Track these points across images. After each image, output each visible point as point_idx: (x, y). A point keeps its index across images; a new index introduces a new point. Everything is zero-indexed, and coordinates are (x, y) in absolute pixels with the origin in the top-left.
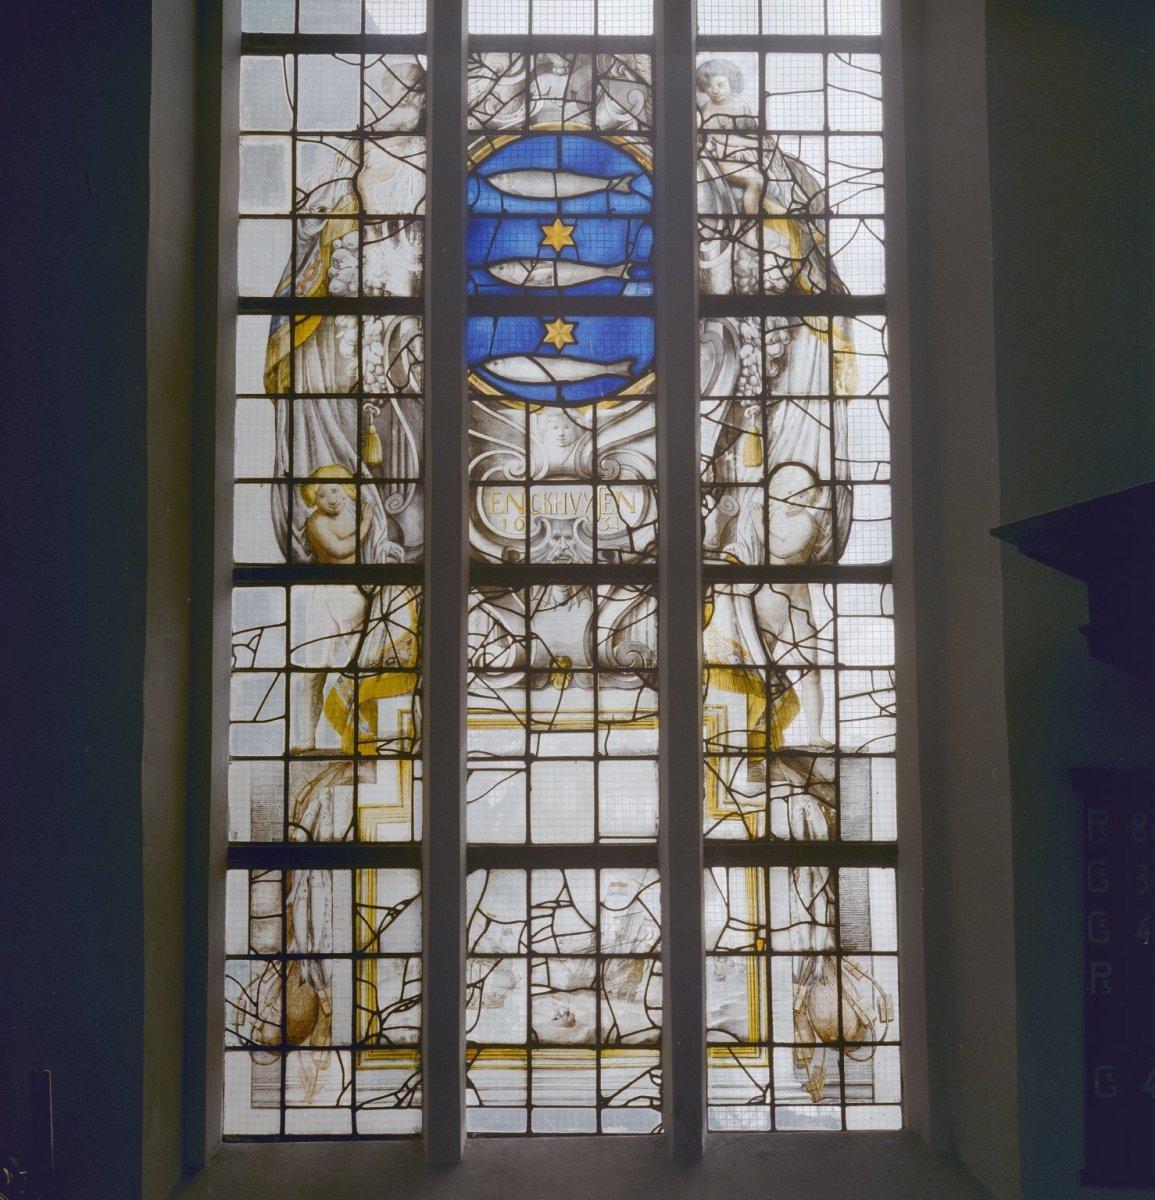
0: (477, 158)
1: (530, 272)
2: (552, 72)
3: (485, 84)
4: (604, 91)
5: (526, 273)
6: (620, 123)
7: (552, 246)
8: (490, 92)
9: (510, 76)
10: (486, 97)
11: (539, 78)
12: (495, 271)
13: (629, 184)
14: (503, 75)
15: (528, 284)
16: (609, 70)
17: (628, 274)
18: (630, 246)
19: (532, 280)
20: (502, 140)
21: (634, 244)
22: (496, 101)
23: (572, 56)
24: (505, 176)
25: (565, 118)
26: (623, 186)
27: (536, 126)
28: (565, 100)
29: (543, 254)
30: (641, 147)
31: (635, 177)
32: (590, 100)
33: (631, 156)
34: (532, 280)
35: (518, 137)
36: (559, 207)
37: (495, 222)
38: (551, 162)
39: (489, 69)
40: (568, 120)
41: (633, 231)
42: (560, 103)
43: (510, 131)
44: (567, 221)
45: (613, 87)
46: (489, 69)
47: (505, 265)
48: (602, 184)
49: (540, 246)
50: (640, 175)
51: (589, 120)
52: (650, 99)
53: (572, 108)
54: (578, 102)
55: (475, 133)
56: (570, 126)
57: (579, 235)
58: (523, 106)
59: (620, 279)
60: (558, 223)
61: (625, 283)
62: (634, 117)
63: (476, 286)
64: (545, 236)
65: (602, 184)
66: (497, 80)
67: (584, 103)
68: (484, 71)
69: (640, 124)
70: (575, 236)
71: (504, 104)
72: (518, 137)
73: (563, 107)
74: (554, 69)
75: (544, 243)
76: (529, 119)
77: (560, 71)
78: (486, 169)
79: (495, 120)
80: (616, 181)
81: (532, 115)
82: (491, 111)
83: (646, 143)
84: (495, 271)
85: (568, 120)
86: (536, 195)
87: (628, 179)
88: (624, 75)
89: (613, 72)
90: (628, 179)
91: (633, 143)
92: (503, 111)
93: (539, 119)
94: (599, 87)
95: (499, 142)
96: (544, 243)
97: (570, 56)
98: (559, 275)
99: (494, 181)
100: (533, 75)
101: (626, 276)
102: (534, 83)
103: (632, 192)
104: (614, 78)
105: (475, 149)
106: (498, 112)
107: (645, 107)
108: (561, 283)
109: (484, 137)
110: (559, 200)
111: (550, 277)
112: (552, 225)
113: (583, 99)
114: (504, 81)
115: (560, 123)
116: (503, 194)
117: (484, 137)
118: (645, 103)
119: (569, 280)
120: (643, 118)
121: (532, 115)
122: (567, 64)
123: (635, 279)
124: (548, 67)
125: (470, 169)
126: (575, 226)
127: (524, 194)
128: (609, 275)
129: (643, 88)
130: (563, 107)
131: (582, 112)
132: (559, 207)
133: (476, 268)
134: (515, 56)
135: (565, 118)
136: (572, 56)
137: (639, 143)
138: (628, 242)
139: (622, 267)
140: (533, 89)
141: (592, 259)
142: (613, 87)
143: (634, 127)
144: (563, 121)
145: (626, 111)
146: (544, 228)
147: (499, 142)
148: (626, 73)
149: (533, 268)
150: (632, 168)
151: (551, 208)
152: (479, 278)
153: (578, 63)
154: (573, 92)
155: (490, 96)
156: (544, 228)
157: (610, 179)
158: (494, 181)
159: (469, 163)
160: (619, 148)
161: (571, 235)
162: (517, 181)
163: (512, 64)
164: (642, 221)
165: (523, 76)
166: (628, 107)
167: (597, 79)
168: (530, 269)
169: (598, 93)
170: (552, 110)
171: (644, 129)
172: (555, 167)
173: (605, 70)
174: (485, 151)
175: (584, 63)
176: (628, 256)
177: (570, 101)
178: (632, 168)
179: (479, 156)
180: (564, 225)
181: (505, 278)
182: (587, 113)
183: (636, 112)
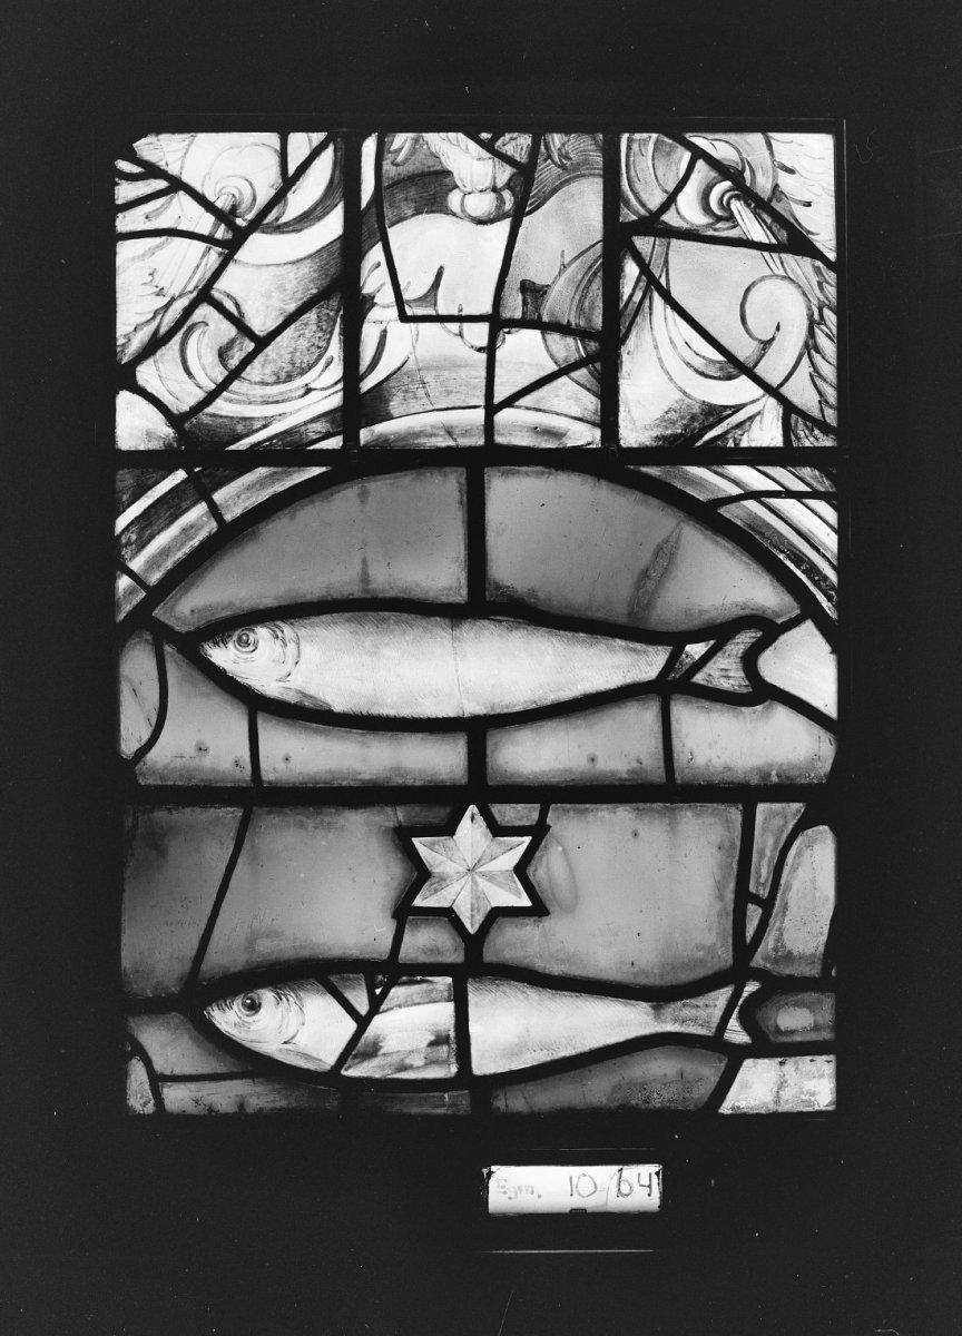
0: (153, 564)
1: (363, 1022)
2: (446, 211)
3: (183, 264)
4: (652, 283)
5: (350, 1026)
6: (715, 414)
7: (448, 915)
8: (205, 295)
9: (279, 229)
10: (188, 311)
11: (395, 234)
12: (228, 1018)
13: (749, 661)
14: (255, 225)
15: (354, 1071)
16: (671, 199)
17: (747, 1023)
18: (754, 914)
19: (372, 1051)
20: (262, 483)
21: (767, 905)
22: (230, 330)
23: (525, 140)
24: (262, 633)
25: (498, 398)
26: (724, 671)
27: (382, 428)
28: (497, 323)
29: (422, 942)
30: (789, 506)
31: (769, 630)
32: (598, 321)
33: (757, 547)
34: (372, 1051)
35: (316, 471)
36: (477, 757)
37: (231, 815)
38: (443, 575)
39: (200, 199)
40: (510, 402)
41: (765, 844)
42: (479, 334)
43: (288, 450)
44: (508, 813)
45: (686, 267)
46: (200, 199)
47: (267, 996)
48: (648, 664)
49: (404, 912)
50: (794, 623)
51: (590, 403)
52: (831, 317)
53: (525, 353)
54: (546, 327)
55: (151, 463)
56: (515, 426)
57: (552, 867)
58: (335, 349)
59: (714, 1043)
60: (471, 829)
61: (735, 1057)
62: (772, 391)
63: (157, 1080)
64: (420, 875)
65: (648, 664)
66: (230, 247)
67: (565, 330)
68: (183, 212)
69: (789, 409)
70: (538, 873)
71: (262, 343)
72: (316, 471)
73: (490, 350)
74: (454, 200)
75: (418, 902)
76: (359, 405)
77: (483, 204)
78: (189, 607)
79: (221, 407)
80: (696, 650)
81: (367, 385)
82: (209, 371)
83: (815, 495)
84: (228, 1018)
85: (510, 402)
86: (392, 704)
87: (745, 639)
88: (731, 218)
89: (688, 211)
90: (745, 639)
91: (757, 495)
92: (254, 371)
93: (395, 406)
94: (631, 269)
95: (235, 497)
96: (418, 902)
97: (517, 144)
98: (474, 1028)
99: (223, 656)
100: (373, 221)
101: (736, 1034)
102: (376, 254)
103: (761, 693)
104: (691, 235)
105: (149, 524)
106: (235, 374)
107: (810, 346)
108: (482, 1065)
109: (180, 475)
110: (478, 730)
111: (439, 1041)
112: (448, 829)
113: (569, 316)
114: (258, 246)
115: (479, 416)
116: (256, 705)
117: (180, 475)
118: (811, 333)
119: (516, 1051)
120: (802, 393)
121: (367, 385)
122: (505, 174)
123: (769, 1045)
124: (431, 190)
125: (126, 608)
126: (539, 832)
127: (339, 706)
128: (670, 1028)
129: (801, 267)
130: (490, 350)
131: (565, 371)
132: (477, 757)
133: (157, 1006)
134: (300, 144)
135: (498, 399)
136: (525, 140)
137: (788, 494)
138: (743, 897)
139: (722, 997)
140: (373, 279)
141: (604, 961)
142: (686, 267)
143: (767, 432)
144: (492, 409)
145: (735, 367)
146: (416, 841)
147: (235, 497)
148: (737, 206)
149: (376, 1005)
150: (763, 594)
151: (444, 760)
152: (166, 1045)
153: (546, 172)
154: (532, 291)
155: (204, 312)
156: (416, 841)
157: (675, 640)
158: (223, 656)
159: (124, 582)
160: (709, 515)
161: (521, 870)
162: (311, 652)
163: (288, 182)
164: (797, 807)
165: (332, 226)
166: (744, 350)
167: (619, 237)
168: (363, 1008)
169: (626, 290)
170: (454, 365)
171: (808, 439)
172: (461, 596)
173: (655, 200)
174: (187, 532)
175: (572, 172)
176: (743, 949)
177: (524, 323)
178: (763, 594)
179: (165, 552)
180: (497, 830)
181: (271, 1047)
182: (582, 374)
183: (772, 370)
